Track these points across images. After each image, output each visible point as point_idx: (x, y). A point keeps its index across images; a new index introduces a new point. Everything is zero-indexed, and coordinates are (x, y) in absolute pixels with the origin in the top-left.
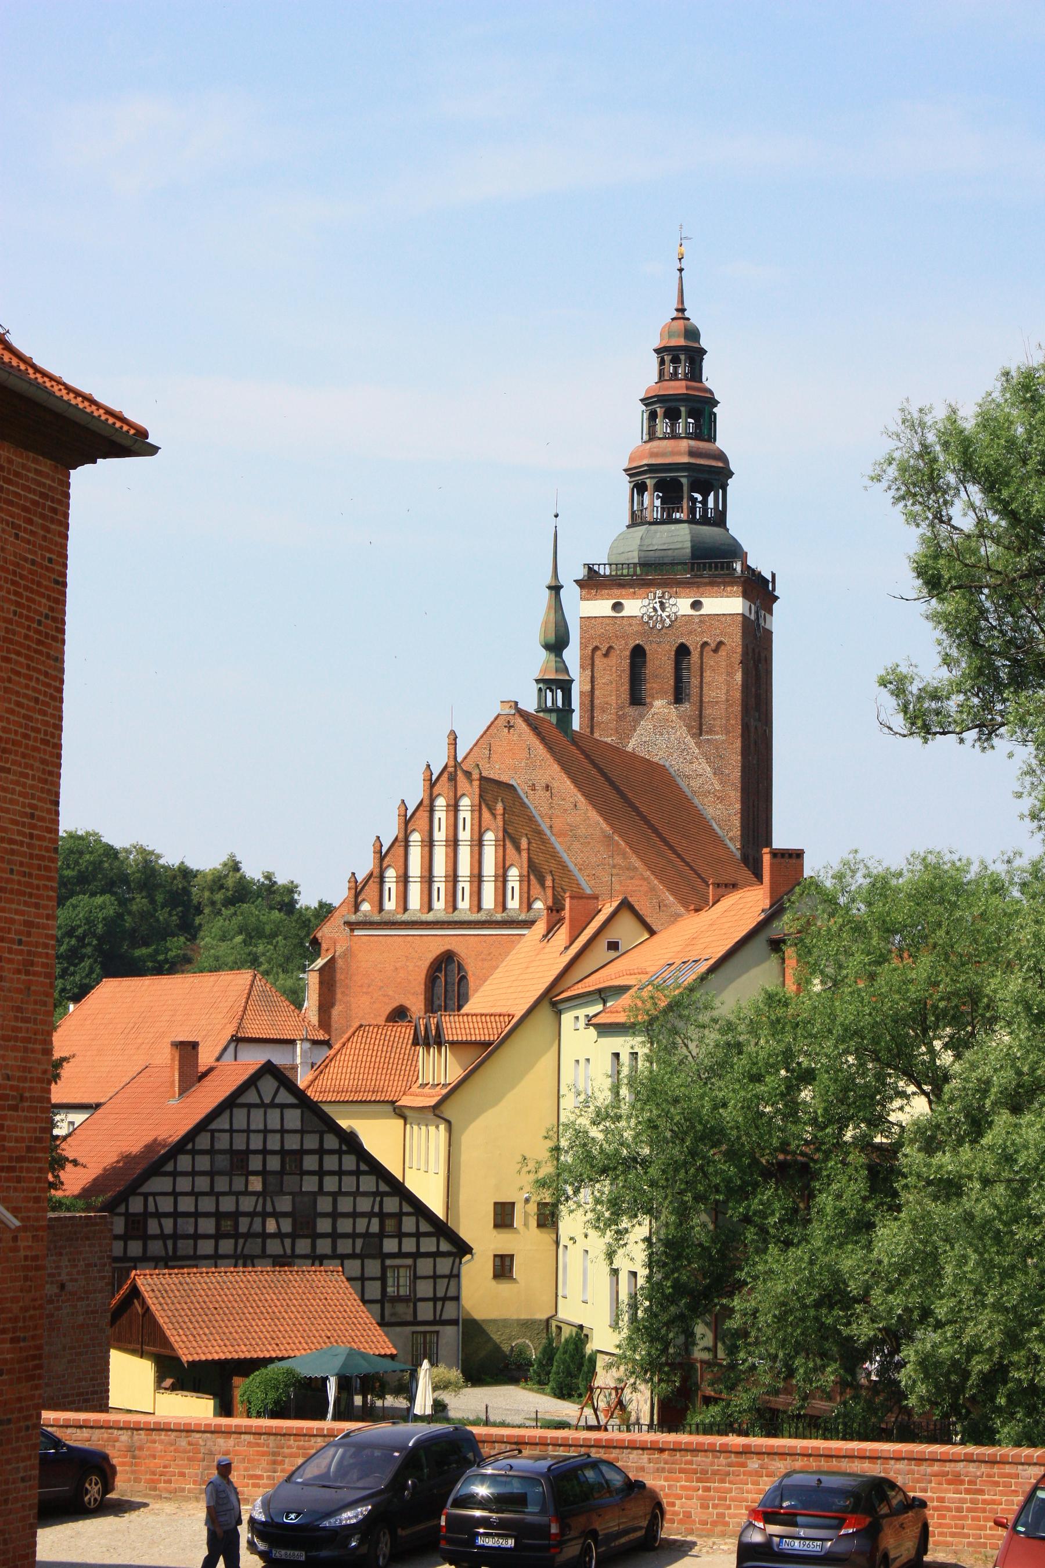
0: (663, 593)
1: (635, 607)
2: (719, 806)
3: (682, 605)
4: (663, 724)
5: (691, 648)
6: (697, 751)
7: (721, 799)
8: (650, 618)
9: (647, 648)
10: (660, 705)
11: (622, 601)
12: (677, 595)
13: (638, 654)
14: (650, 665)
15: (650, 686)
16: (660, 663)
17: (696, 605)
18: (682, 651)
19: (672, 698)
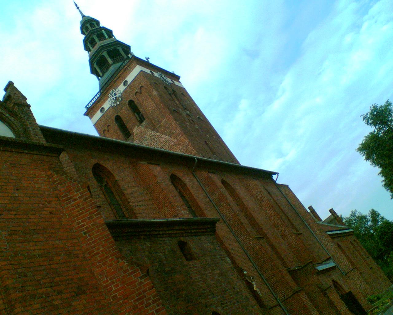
0: (113, 90)
1: (107, 106)
2: (181, 147)
3: (121, 88)
4: (141, 135)
5: (133, 100)
6: (158, 134)
7: (180, 144)
8: (114, 103)
9: (119, 114)
10: (136, 130)
11: (102, 107)
12: (117, 87)
13: (118, 119)
14: (123, 119)
15: (129, 126)
16: (127, 114)
17: (125, 83)
18: (131, 104)
19: (138, 123)
